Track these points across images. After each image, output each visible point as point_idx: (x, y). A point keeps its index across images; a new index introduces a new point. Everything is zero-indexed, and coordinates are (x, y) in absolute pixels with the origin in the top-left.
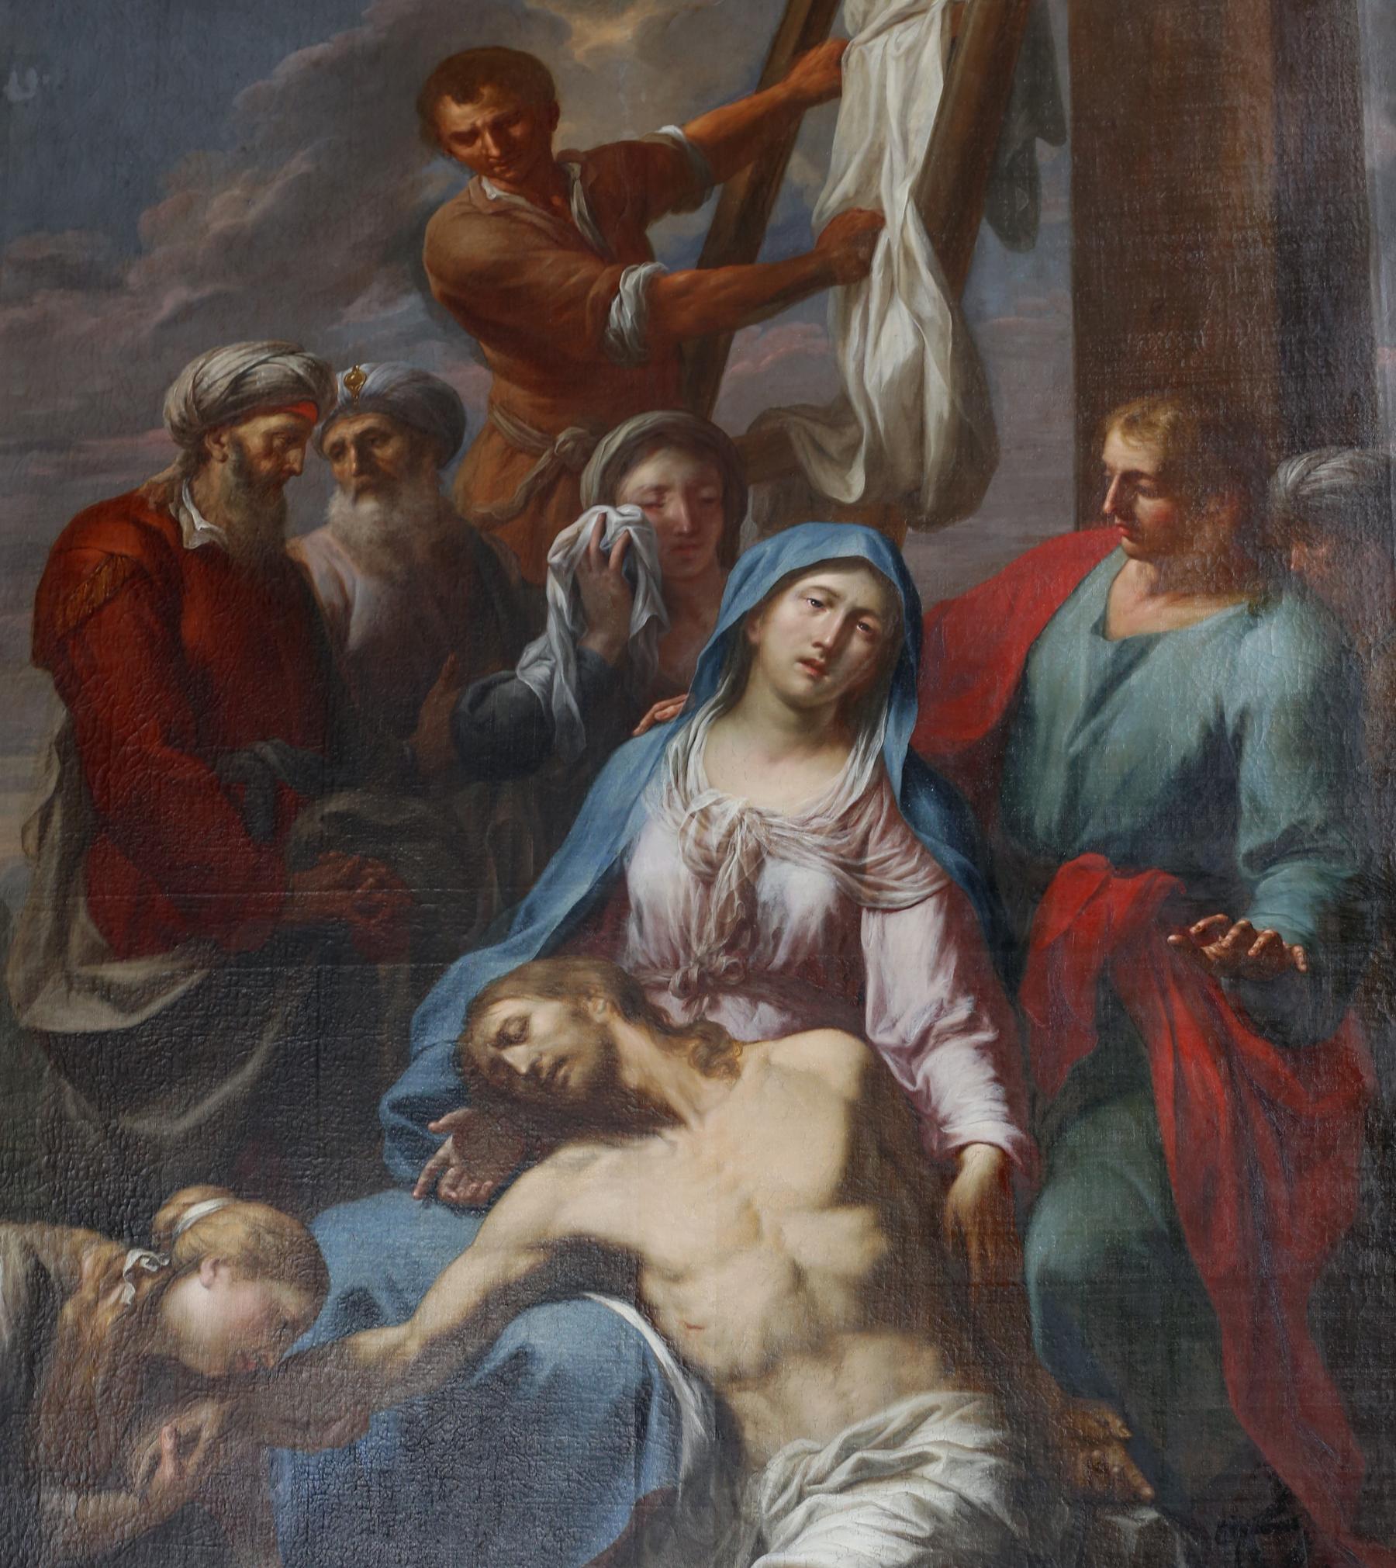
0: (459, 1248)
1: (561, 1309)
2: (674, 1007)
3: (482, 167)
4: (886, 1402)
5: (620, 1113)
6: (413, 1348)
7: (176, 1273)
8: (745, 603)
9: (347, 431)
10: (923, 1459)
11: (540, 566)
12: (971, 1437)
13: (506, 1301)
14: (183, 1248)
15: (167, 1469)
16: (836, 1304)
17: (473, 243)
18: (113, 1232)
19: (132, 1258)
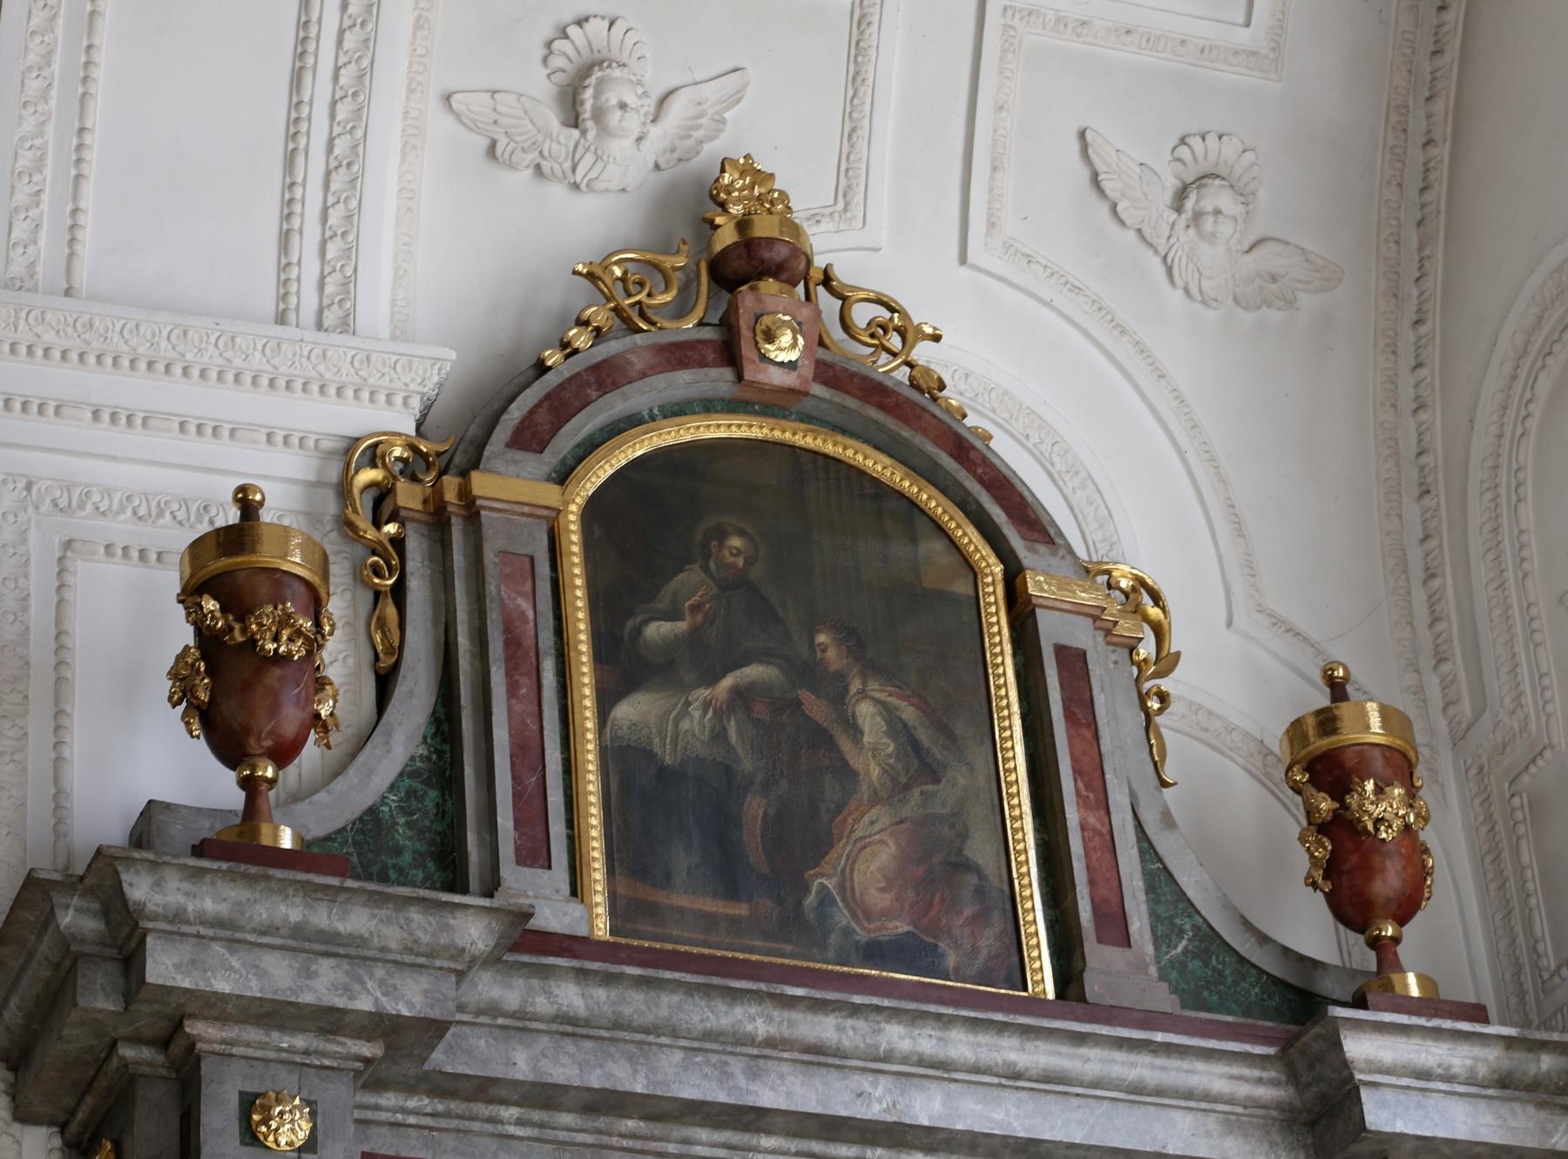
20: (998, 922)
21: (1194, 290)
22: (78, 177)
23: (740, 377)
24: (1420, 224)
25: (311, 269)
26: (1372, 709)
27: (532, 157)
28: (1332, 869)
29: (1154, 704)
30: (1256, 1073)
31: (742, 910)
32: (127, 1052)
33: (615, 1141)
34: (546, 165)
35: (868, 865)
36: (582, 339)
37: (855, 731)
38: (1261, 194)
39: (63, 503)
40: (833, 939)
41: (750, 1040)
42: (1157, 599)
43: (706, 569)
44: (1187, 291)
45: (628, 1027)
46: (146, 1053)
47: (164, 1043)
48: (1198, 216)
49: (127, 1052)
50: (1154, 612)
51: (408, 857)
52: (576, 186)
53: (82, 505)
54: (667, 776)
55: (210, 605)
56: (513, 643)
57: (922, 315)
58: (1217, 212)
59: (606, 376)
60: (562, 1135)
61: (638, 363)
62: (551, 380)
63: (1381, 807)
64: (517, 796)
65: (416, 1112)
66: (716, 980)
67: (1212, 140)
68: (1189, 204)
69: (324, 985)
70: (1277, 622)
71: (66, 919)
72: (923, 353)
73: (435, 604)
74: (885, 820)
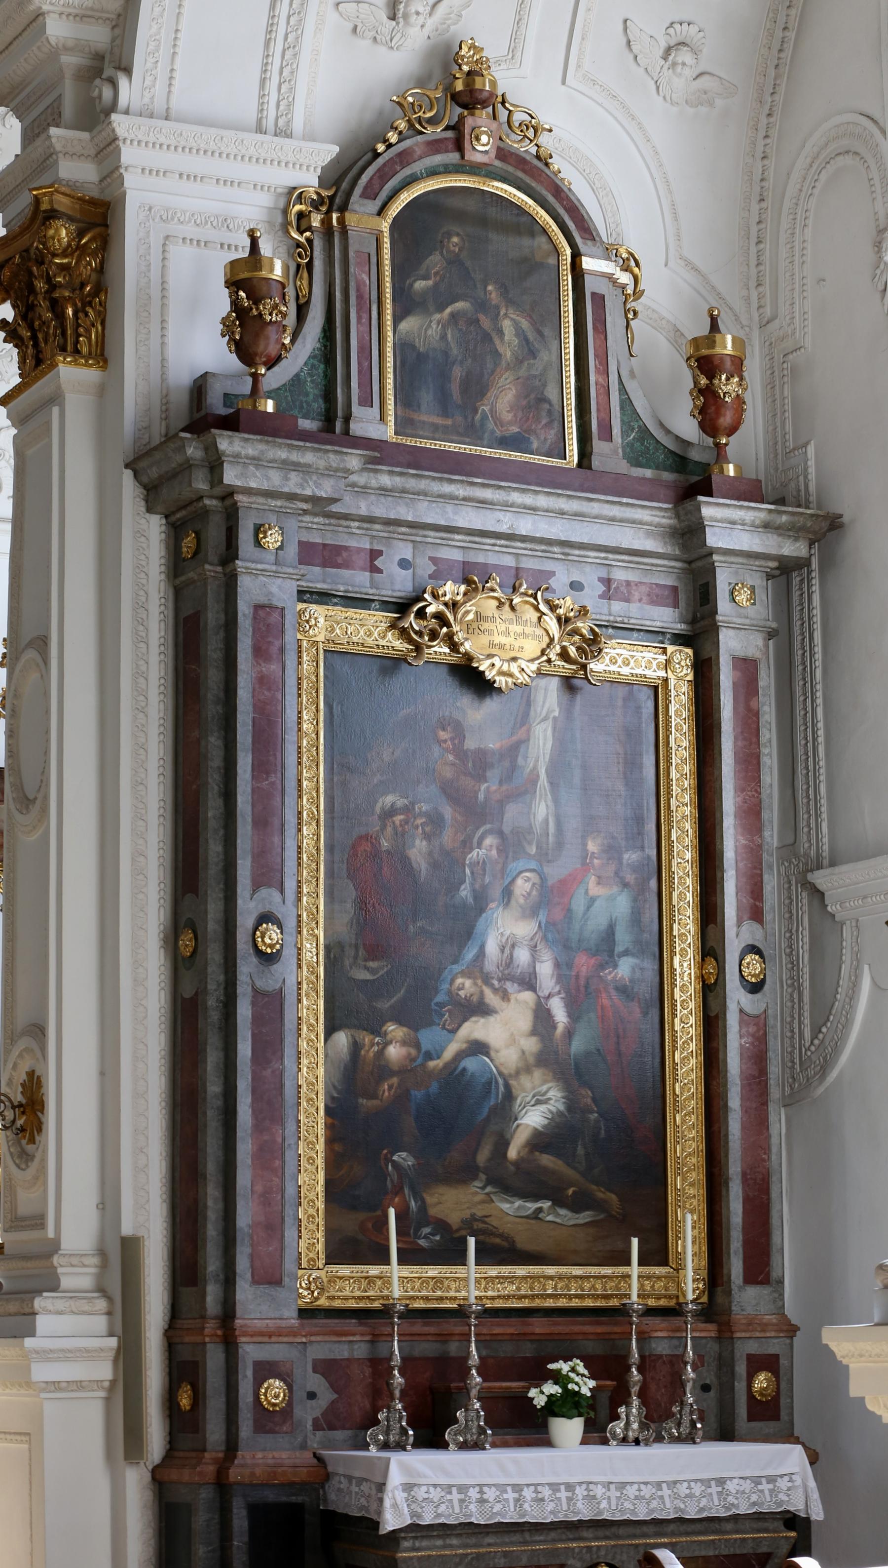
0: (450, 1041)
1: (471, 1058)
2: (496, 982)
3: (447, 750)
4: (542, 1085)
5: (481, 1009)
6: (441, 1065)
7: (387, 1044)
8: (509, 879)
9: (419, 821)
10: (550, 1099)
11: (464, 865)
12: (559, 1095)
13: (459, 1056)
14: (389, 1037)
15: (386, 1094)
16: (531, 1060)
17: (448, 773)
18: (372, 1033)
19: (377, 1040)
20: (556, 424)
21: (668, 98)
22: (174, 53)
23: (463, 157)
24: (777, 66)
25: (273, 97)
26: (729, 338)
27: (373, 33)
28: (703, 411)
29: (630, 316)
30: (662, 514)
31: (449, 422)
32: (207, 502)
33: (395, 536)
34: (378, 37)
35: (503, 400)
36: (393, 137)
37: (501, 333)
38: (705, 50)
39: (164, 217)
40: (486, 435)
41: (456, 498)
42: (637, 265)
43: (442, 254)
44: (664, 98)
45: (408, 493)
46: (214, 502)
47: (223, 499)
48: (674, 64)
49: (207, 502)
50: (636, 270)
51: (311, 397)
52: (392, 48)
53: (173, 219)
54: (421, 358)
55: (242, 294)
56: (360, 297)
57: (545, 119)
58: (684, 64)
59: (404, 158)
60: (374, 533)
61: (418, 152)
62: (380, 161)
63: (727, 387)
64: (360, 372)
65: (317, 523)
66: (446, 476)
67: (685, 25)
68: (671, 58)
69: (293, 484)
70: (688, 263)
71: (190, 451)
72: (544, 139)
73: (325, 273)
74: (512, 378)
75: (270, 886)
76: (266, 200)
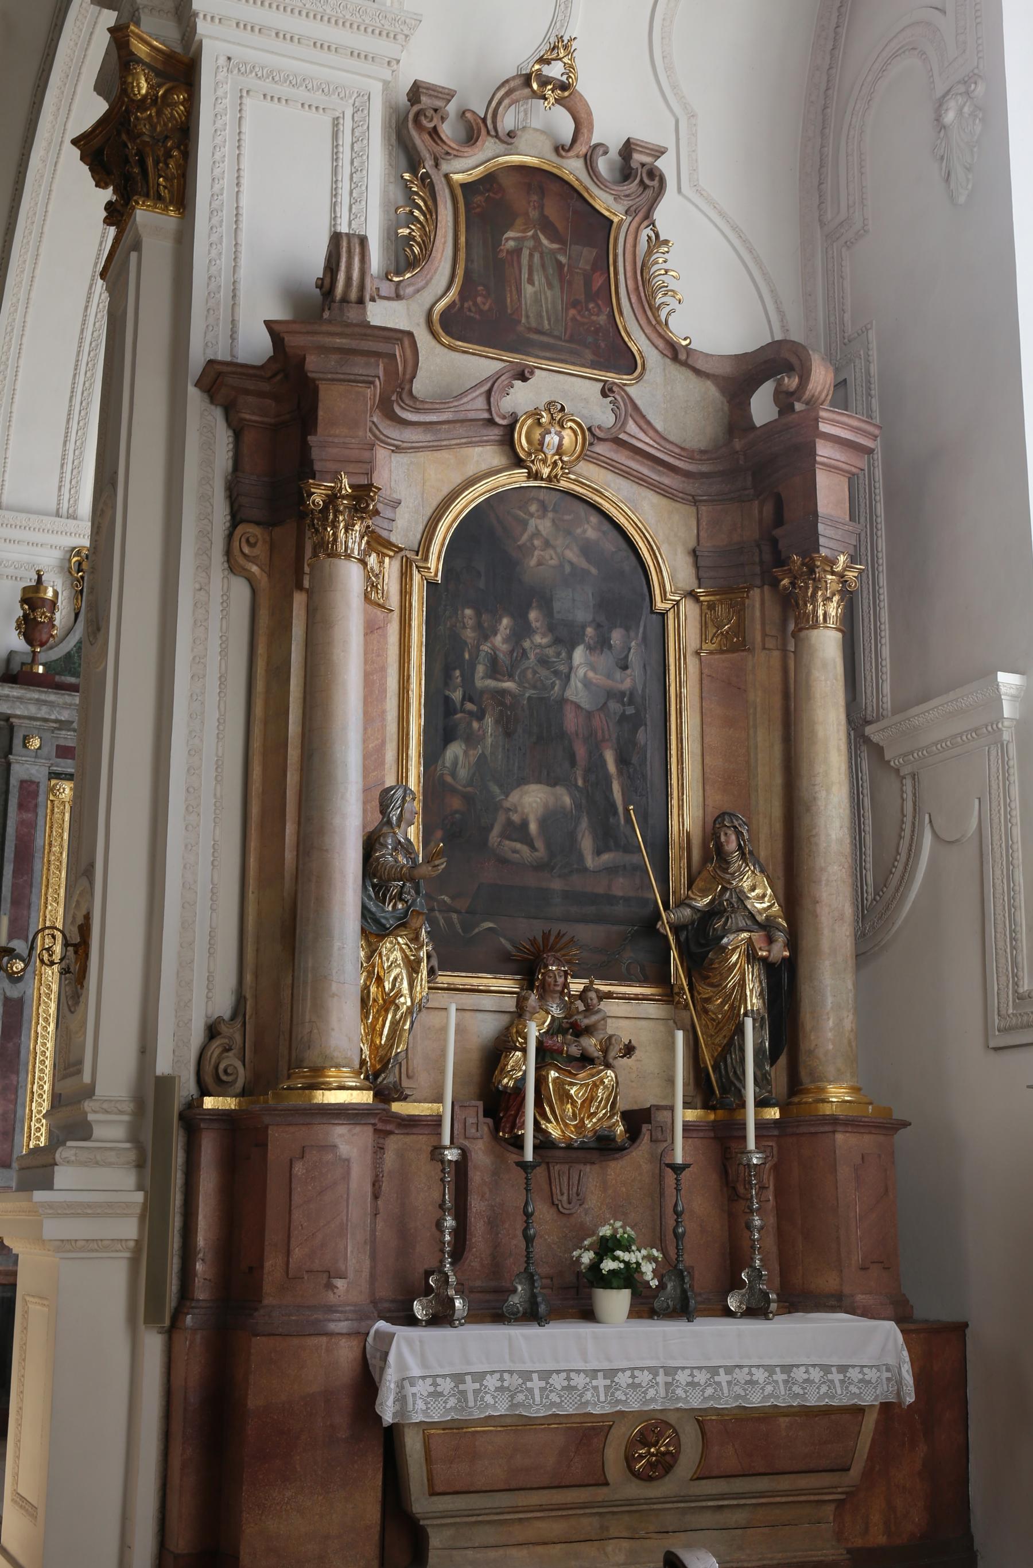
25: (66, 497)
55: (26, 607)
69: (44, 712)
75: (19, 938)
76: (58, 554)
